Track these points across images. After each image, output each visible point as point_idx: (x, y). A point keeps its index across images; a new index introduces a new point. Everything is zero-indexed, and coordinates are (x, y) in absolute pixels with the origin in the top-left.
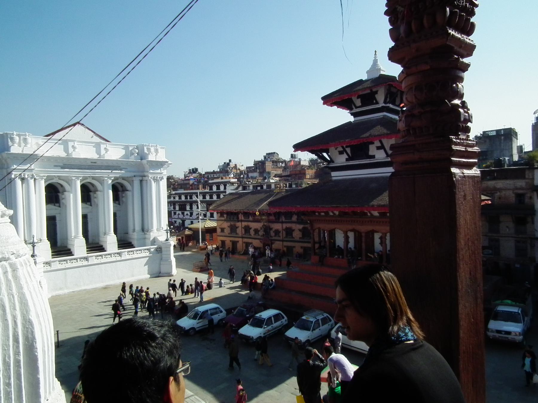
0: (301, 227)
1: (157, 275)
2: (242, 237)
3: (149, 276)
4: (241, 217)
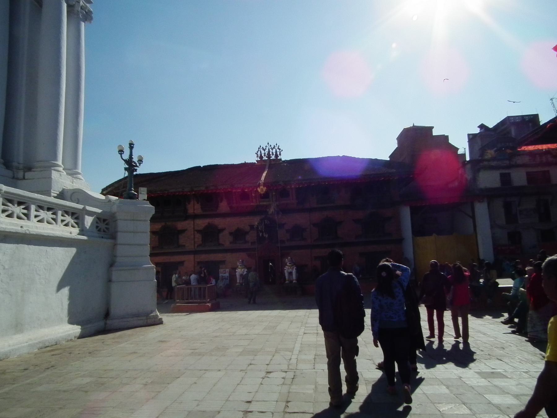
1: (101, 324)
2: (195, 252)
3: (77, 329)
4: (194, 207)
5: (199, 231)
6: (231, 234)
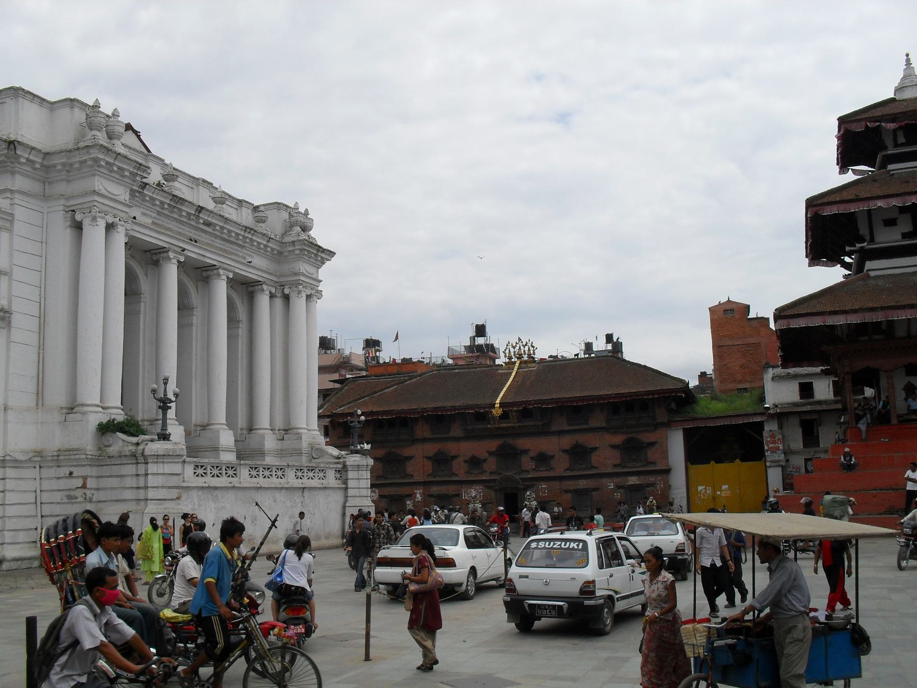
0: (618, 439)
4: (423, 431)
5: (428, 458)
6: (466, 461)
